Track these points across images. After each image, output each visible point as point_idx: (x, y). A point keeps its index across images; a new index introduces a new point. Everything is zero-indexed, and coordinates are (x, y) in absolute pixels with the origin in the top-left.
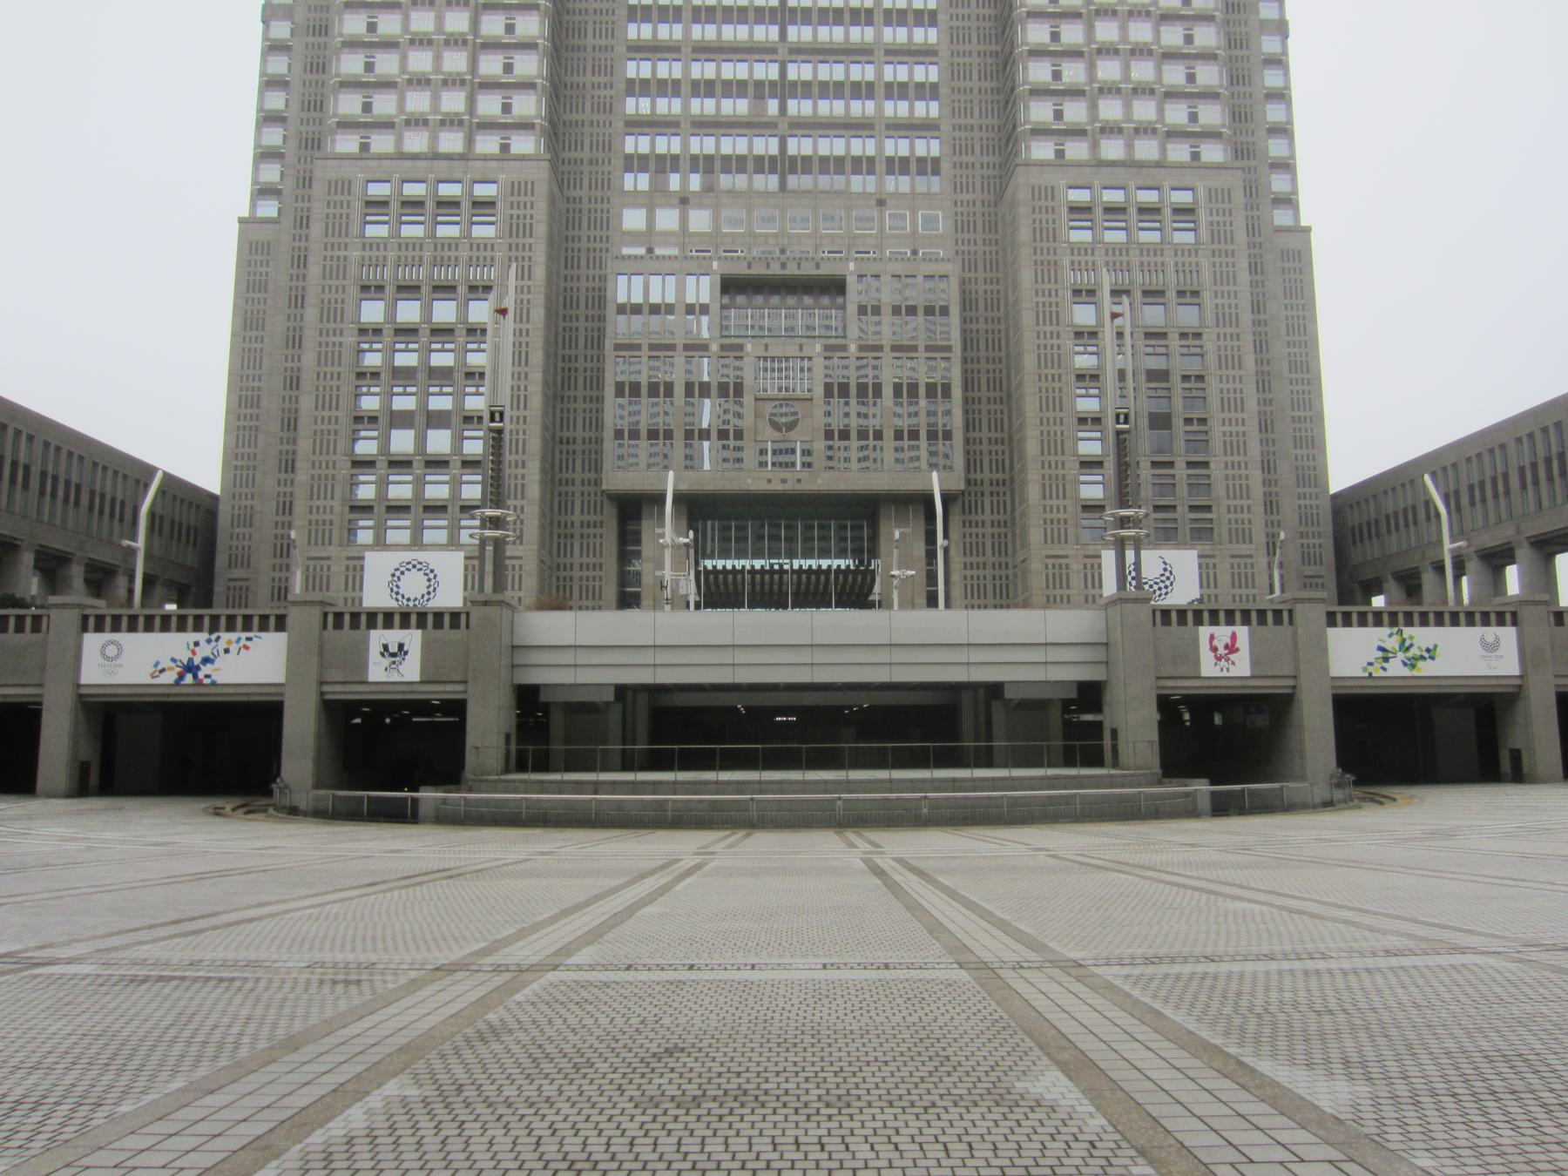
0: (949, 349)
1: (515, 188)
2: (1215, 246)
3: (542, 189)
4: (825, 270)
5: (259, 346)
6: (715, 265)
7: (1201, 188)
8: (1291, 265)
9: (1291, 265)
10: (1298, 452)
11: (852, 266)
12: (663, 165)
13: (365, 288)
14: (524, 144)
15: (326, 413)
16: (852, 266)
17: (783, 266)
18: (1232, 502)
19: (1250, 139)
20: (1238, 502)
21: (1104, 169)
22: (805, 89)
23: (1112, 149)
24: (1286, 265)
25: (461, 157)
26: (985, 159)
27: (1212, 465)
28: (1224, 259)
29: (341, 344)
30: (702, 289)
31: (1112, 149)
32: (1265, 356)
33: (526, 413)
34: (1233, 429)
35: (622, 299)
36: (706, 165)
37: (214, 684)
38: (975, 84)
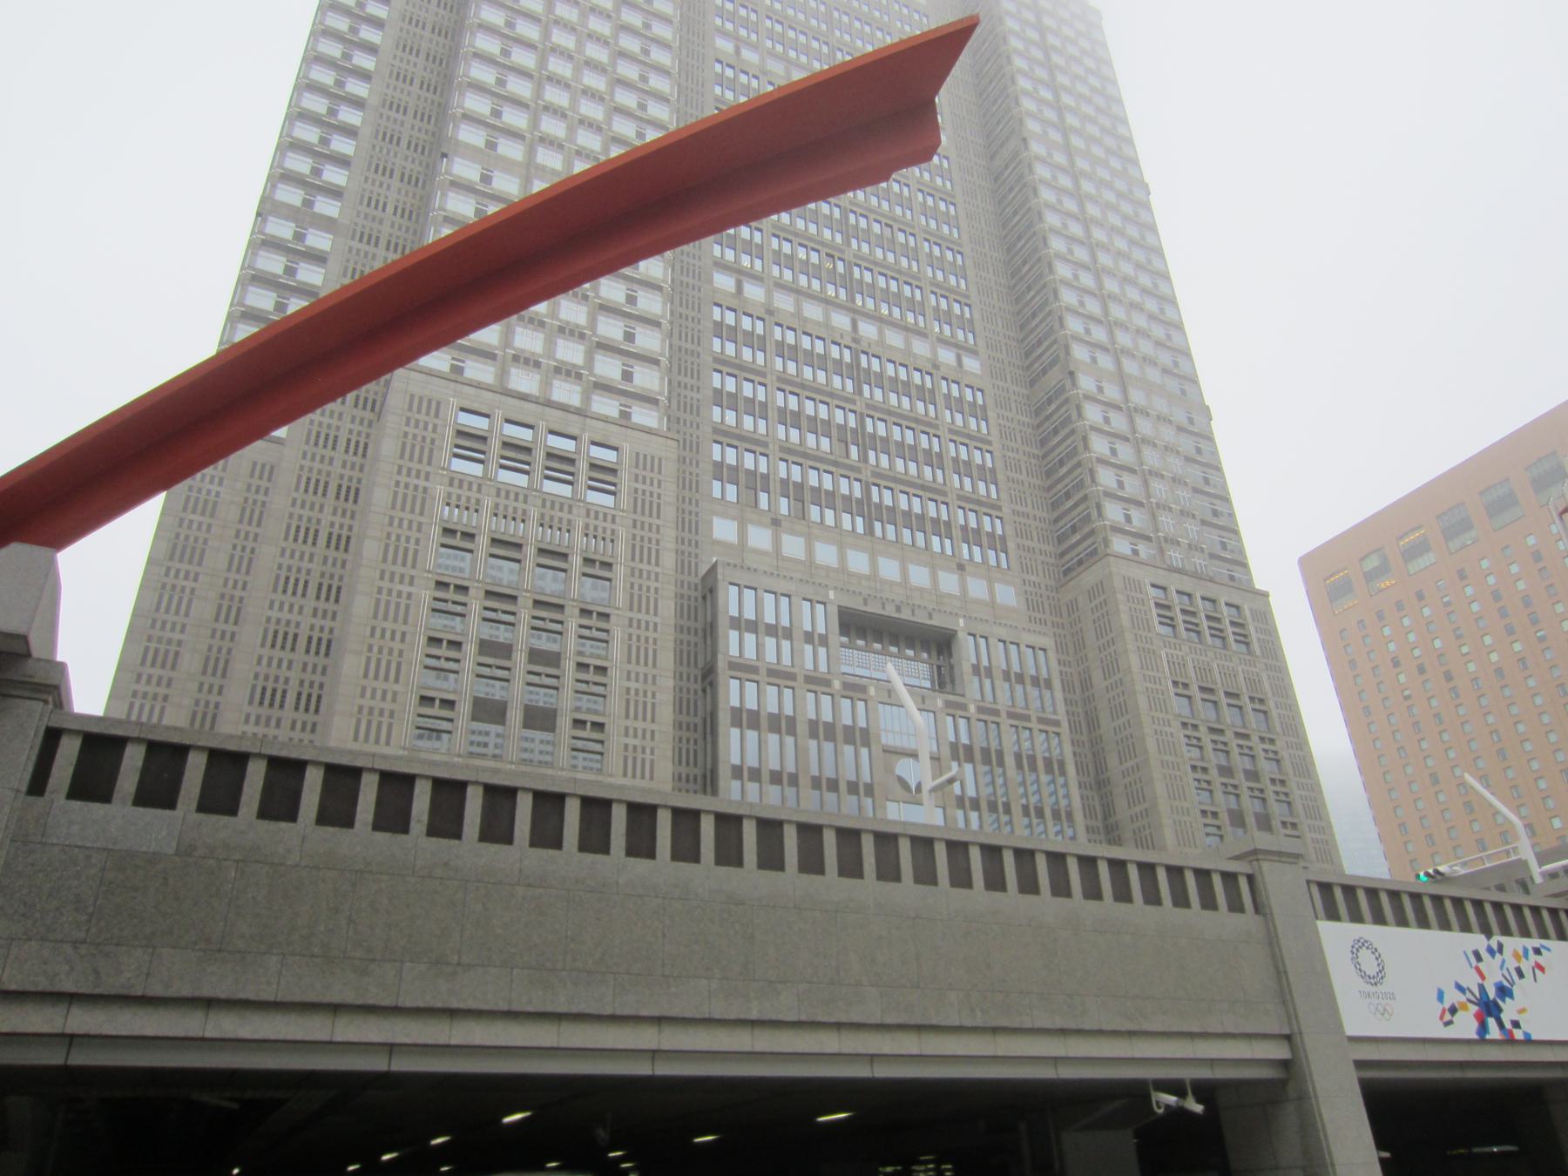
0: (1057, 723)
1: (639, 460)
3: (670, 469)
4: (937, 621)
5: (189, 584)
6: (831, 594)
12: (755, 483)
13: (448, 532)
14: (643, 416)
15: (380, 685)
16: (961, 621)
17: (898, 609)
22: (885, 445)
25: (578, 412)
26: (1043, 547)
29: (409, 596)
30: (820, 620)
33: (654, 727)
35: (734, 612)
36: (797, 493)
37: (1528, 1041)
38: (1023, 477)
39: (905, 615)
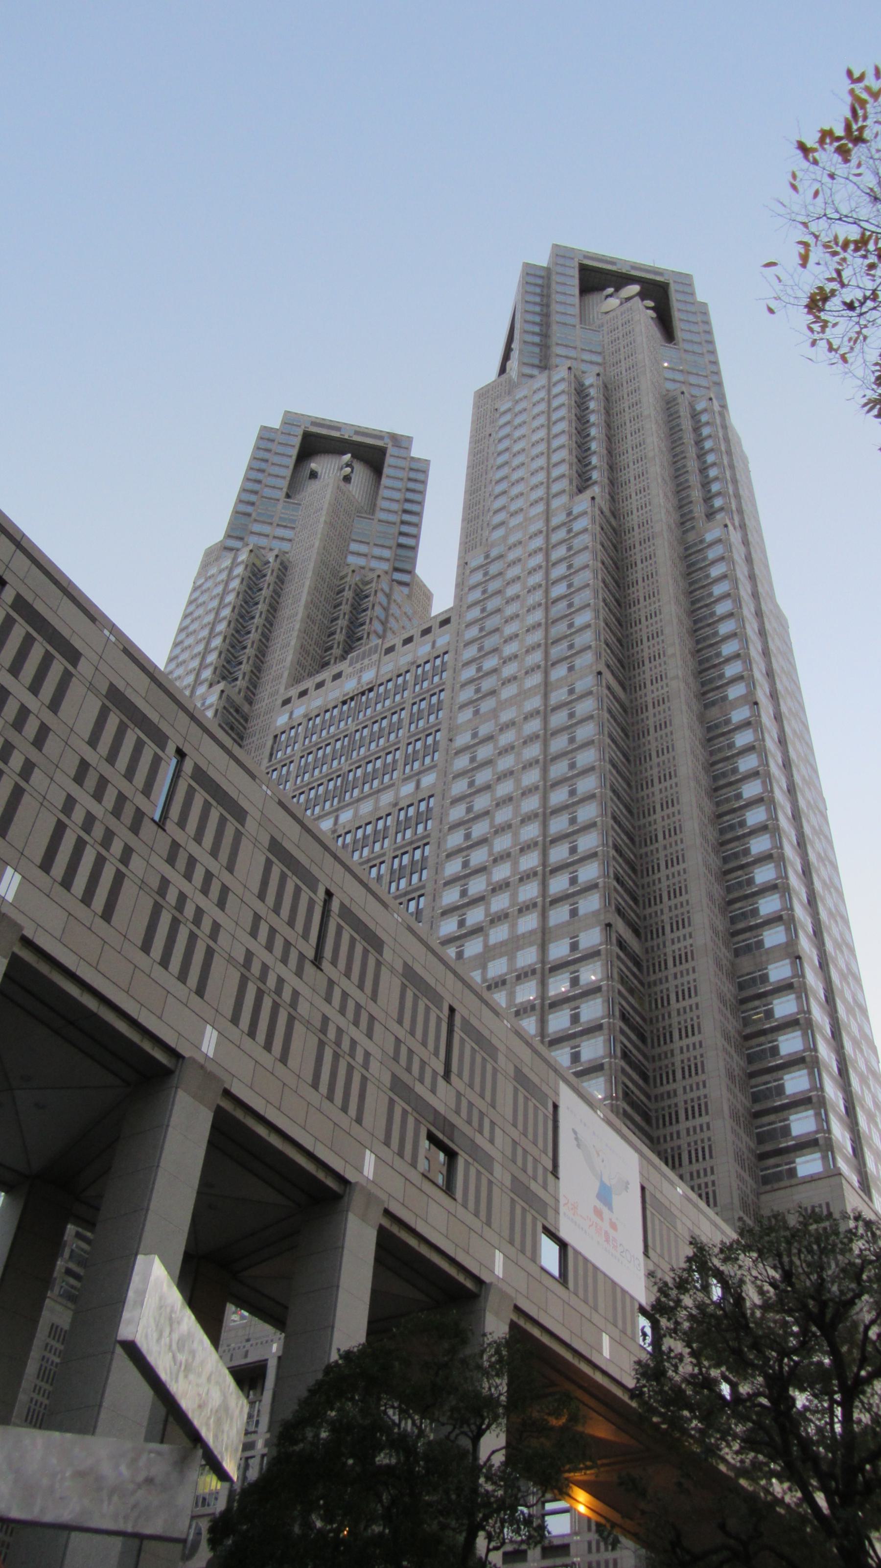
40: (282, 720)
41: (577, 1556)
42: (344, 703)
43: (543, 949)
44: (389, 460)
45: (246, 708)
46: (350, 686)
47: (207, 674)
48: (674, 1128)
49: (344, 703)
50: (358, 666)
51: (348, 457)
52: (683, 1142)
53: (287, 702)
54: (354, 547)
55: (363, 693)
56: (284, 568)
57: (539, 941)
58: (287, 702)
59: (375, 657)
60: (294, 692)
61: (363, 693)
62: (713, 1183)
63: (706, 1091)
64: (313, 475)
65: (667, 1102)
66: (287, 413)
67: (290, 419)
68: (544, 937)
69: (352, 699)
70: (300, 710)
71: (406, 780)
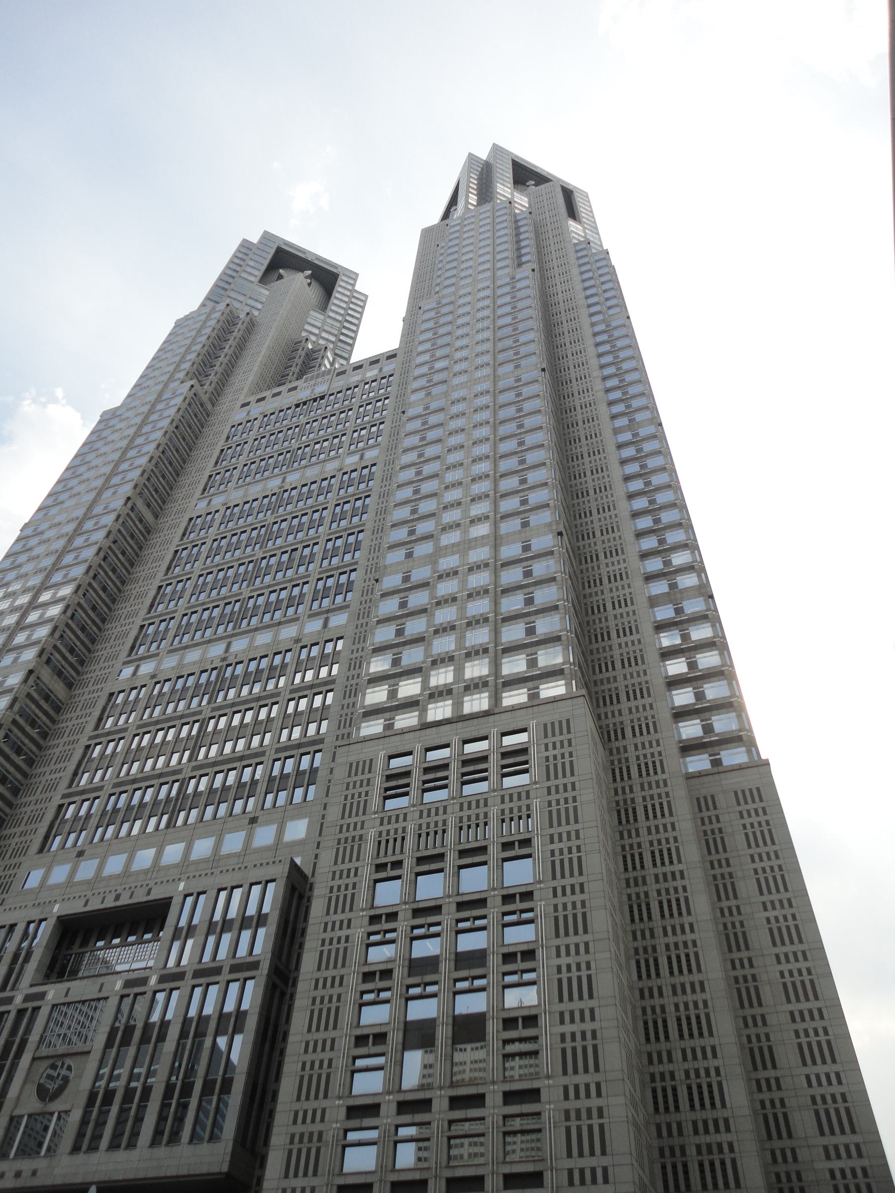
2: (553, 783)
7: (532, 724)
8: (751, 806)
9: (751, 806)
10: (811, 1070)
11: (181, 886)
17: (117, 898)
18: (577, 1163)
19: (643, 679)
20: (587, 1162)
21: (428, 731)
23: (440, 711)
24: (744, 808)
27: (544, 1095)
28: (561, 796)
31: (440, 711)
32: (686, 920)
34: (576, 1028)
39: (124, 901)
40: (240, 415)
41: (549, 1103)
42: (297, 406)
43: (496, 548)
44: (340, 282)
45: (209, 406)
46: (303, 394)
47: (181, 375)
48: (616, 708)
49: (297, 406)
50: (312, 382)
51: (309, 272)
52: (626, 718)
53: (244, 405)
54: (307, 327)
55: (315, 400)
56: (252, 326)
57: (492, 543)
58: (244, 405)
59: (327, 377)
60: (253, 399)
61: (315, 400)
62: (660, 754)
63: (647, 678)
64: (280, 277)
65: (606, 687)
66: (266, 232)
67: (267, 237)
68: (496, 541)
69: (305, 403)
70: (256, 410)
71: (351, 453)
